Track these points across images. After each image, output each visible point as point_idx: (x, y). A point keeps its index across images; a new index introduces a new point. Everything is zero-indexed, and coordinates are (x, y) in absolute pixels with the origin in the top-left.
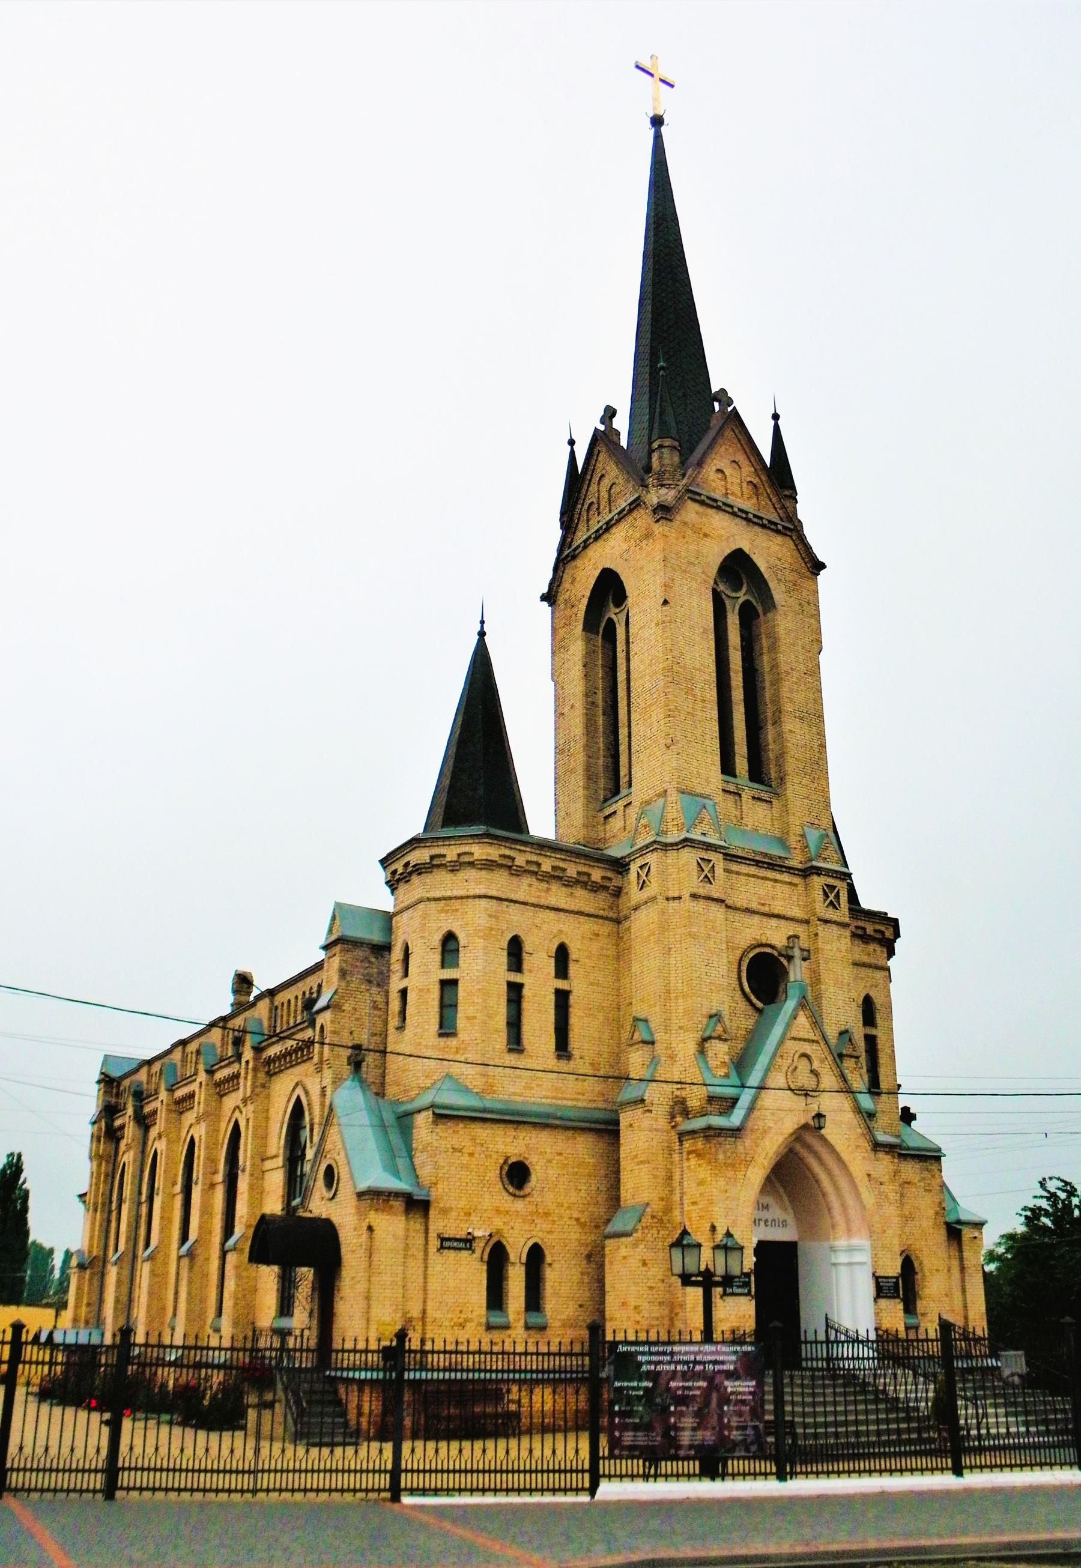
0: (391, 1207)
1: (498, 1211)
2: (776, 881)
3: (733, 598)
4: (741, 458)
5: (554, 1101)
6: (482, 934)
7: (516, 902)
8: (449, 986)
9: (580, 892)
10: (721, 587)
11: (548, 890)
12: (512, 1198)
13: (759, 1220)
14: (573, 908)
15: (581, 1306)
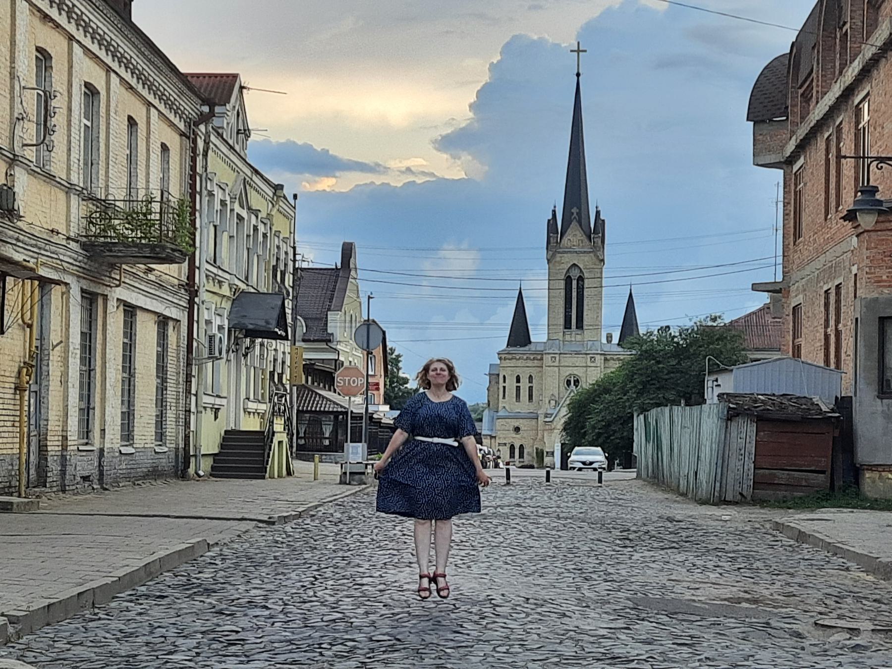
4: (577, 233)
8: (504, 387)
9: (536, 361)
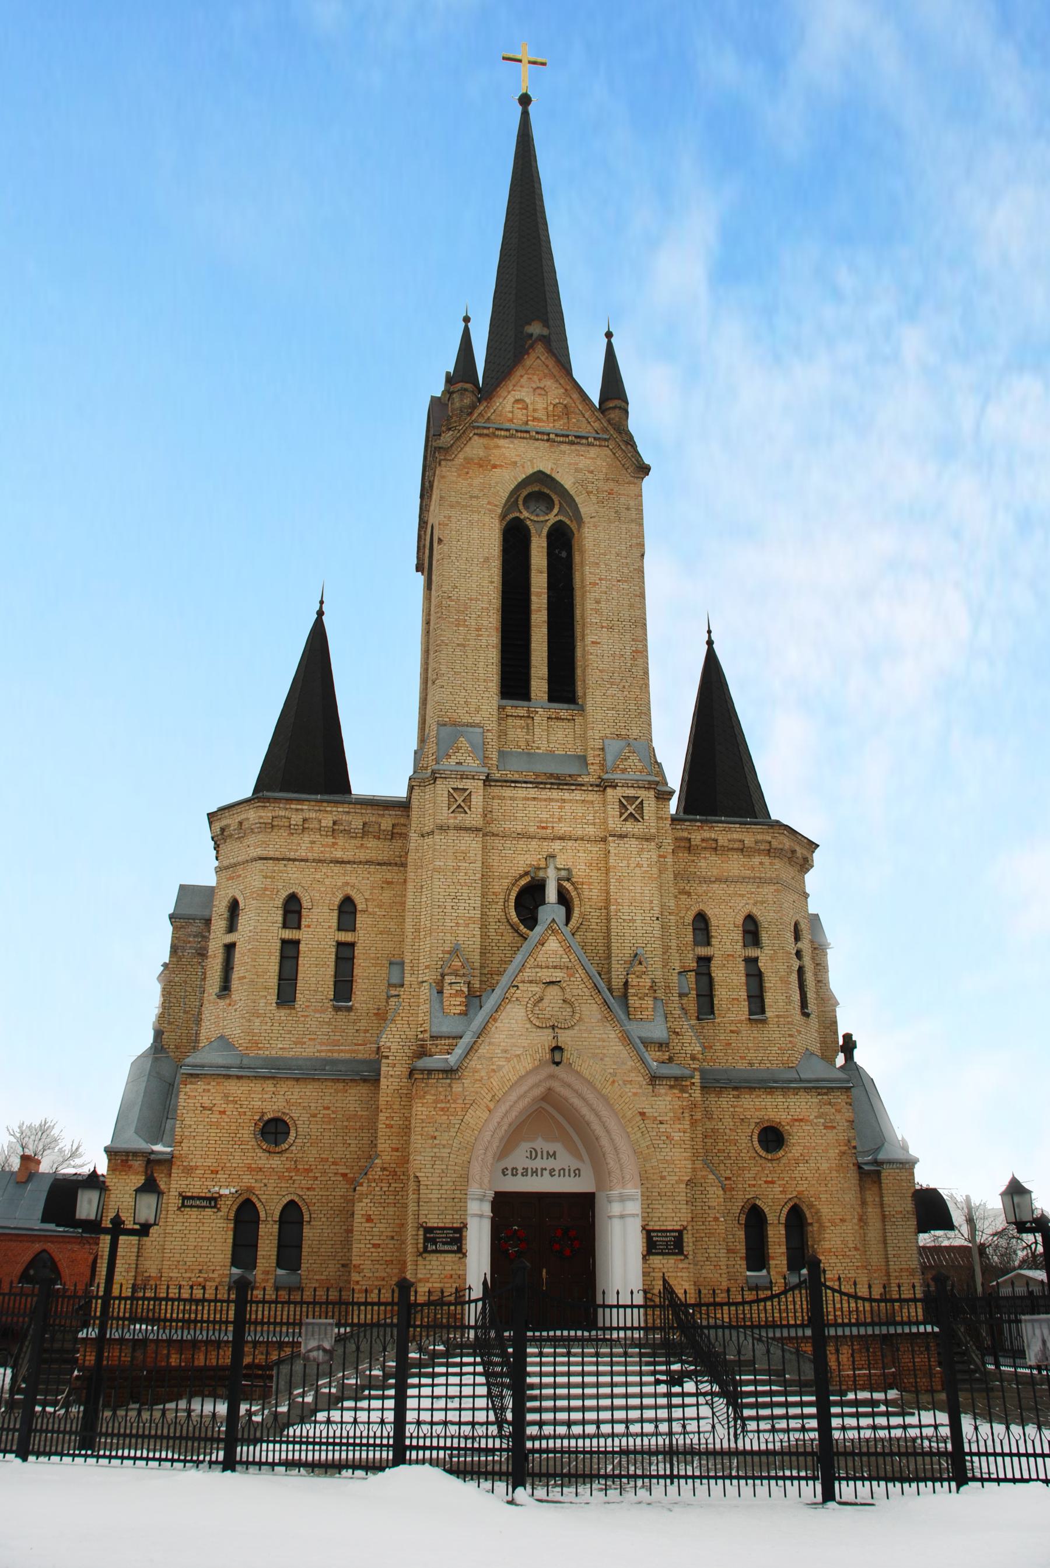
0: (130, 1167)
1: (250, 1169)
2: (564, 801)
3: (542, 521)
4: (549, 383)
5: (330, 1054)
6: (255, 895)
7: (294, 860)
9: (371, 843)
10: (525, 514)
11: (336, 844)
12: (268, 1154)
13: (542, 1169)
14: (363, 858)
15: (343, 1266)
